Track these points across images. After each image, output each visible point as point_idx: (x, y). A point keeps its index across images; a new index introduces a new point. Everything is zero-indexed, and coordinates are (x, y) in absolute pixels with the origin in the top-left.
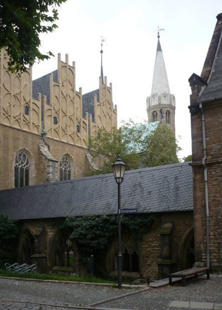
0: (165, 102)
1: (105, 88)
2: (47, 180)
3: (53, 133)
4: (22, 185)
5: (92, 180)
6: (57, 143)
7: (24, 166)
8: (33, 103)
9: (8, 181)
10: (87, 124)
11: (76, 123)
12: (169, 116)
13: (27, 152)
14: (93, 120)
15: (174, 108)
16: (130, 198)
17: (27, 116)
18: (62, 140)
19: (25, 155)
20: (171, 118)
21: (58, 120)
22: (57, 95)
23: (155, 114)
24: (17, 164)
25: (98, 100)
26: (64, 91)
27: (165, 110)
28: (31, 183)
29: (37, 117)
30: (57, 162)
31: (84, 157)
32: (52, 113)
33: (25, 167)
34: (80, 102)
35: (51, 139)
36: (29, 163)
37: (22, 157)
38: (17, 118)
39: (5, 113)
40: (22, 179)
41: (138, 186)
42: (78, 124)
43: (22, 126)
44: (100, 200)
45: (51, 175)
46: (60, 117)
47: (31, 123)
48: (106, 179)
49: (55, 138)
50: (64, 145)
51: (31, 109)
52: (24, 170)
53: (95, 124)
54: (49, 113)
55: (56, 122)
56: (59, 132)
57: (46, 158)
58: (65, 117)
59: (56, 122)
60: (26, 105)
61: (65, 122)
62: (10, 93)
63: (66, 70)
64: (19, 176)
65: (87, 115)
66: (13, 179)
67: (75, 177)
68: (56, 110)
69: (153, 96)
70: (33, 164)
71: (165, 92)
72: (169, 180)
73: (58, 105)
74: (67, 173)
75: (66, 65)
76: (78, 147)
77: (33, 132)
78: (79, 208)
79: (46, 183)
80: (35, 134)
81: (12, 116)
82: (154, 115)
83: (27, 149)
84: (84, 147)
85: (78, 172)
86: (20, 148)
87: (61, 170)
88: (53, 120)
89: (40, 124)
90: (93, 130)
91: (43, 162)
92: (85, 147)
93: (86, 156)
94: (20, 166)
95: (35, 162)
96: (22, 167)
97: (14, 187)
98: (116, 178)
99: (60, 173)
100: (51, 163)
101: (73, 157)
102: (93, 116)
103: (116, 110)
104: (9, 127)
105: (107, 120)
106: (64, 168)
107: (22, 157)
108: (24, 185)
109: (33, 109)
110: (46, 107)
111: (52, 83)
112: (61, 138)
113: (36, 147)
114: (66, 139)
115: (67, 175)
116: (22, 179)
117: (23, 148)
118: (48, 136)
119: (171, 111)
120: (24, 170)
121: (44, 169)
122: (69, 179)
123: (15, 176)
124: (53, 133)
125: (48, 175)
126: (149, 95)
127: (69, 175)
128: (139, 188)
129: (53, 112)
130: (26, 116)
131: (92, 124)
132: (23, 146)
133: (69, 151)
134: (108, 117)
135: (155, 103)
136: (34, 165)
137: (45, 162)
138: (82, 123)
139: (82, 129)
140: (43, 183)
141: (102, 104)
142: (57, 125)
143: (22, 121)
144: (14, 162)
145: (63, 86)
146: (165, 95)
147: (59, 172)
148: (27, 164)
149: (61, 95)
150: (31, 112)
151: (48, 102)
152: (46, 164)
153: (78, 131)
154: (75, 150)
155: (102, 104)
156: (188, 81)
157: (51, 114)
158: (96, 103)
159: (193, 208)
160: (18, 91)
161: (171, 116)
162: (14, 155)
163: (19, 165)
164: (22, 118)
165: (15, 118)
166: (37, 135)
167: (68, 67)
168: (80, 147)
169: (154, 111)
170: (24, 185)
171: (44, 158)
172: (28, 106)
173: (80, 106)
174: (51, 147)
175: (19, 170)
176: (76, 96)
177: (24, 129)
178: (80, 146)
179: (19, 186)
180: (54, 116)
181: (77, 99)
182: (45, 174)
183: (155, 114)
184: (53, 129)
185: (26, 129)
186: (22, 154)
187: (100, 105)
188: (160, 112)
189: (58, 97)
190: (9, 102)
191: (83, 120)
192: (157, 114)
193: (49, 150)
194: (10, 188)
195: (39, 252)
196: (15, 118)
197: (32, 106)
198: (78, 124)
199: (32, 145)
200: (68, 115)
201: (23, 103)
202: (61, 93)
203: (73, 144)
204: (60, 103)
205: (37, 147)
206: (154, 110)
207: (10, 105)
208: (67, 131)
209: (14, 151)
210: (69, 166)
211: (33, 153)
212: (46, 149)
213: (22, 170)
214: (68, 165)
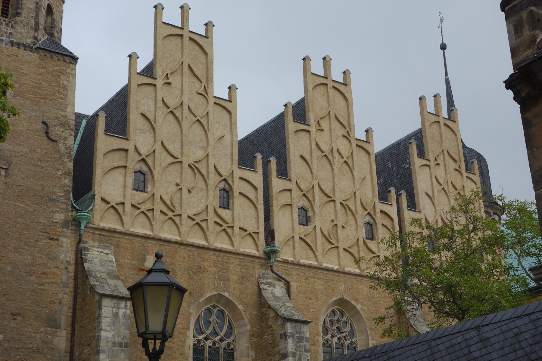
1: (438, 122)
8: (240, 178)
11: (363, 218)
13: (229, 303)
17: (228, 212)
18: (326, 265)
19: (222, 312)
21: (310, 214)
22: (305, 155)
24: (201, 337)
25: (422, 154)
26: (323, 140)
29: (252, 211)
32: (292, 198)
34: (371, 164)
35: (293, 264)
38: (198, 219)
39: (165, 210)
42: (368, 218)
43: (211, 238)
47: (237, 229)
49: (302, 261)
50: (331, 276)
51: (236, 194)
52: (221, 352)
53: (416, 215)
54: (285, 198)
57: (277, 316)
58: (331, 205)
60: (222, 185)
62: (181, 162)
63: (328, 92)
73: (310, 175)
75: (324, 81)
77: (243, 250)
80: (247, 255)
81: (184, 216)
83: (226, 294)
86: (209, 295)
87: (327, 345)
89: (262, 230)
91: (270, 327)
95: (249, 327)
96: (214, 343)
101: (359, 307)
104: (177, 243)
109: (240, 193)
110: (277, 184)
111: (292, 126)
112: (320, 257)
113: (252, 289)
117: (214, 293)
118: (285, 255)
121: (275, 345)
129: (296, 193)
130: (224, 213)
131: (408, 215)
132: (215, 289)
141: (432, 163)
142: (310, 228)
143: (211, 225)
144: (190, 333)
145: (322, 130)
149: (316, 153)
150: (238, 202)
151: (283, 173)
152: (279, 332)
153: (371, 237)
157: (289, 202)
158: (417, 162)
160: (199, 154)
162: (190, 314)
164: (212, 217)
165: (194, 220)
166: (252, 256)
167: (331, 84)
171: (272, 315)
172: (227, 187)
173: (371, 173)
174: (293, 285)
176: (356, 150)
177: (219, 245)
180: (300, 204)
181: (360, 155)
184: (297, 238)
185: (223, 244)
187: (429, 166)
189: (308, 158)
190: (178, 181)
191: (380, 206)
196: (194, 220)
197: (238, 186)
198: (368, 218)
199: (241, 283)
200: (339, 198)
201: (213, 179)
202: (314, 147)
204: (315, 172)
205: (255, 287)
207: (181, 189)
208: (338, 241)
211: (242, 303)
212: (279, 290)
213: (214, 350)
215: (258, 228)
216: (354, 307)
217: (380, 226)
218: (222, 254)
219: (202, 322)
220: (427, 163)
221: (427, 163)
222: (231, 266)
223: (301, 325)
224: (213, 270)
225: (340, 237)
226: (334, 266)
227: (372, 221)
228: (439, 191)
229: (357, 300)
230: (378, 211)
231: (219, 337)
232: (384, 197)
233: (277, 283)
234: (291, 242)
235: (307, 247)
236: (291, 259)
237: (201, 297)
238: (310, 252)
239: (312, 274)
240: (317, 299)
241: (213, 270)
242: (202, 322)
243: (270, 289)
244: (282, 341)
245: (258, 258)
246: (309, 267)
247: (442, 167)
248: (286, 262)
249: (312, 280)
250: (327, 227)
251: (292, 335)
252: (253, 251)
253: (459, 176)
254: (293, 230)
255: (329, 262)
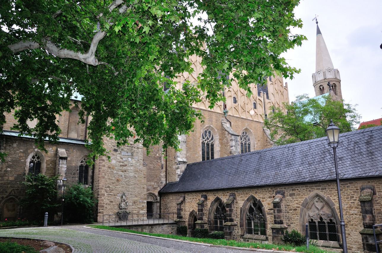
0: (330, 76)
2: (231, 153)
3: (233, 110)
4: (208, 158)
5: (279, 150)
6: (237, 119)
7: (210, 141)
9: (197, 155)
10: (263, 101)
11: (253, 101)
12: (335, 88)
13: (212, 129)
14: (268, 97)
15: (339, 81)
16: (320, 165)
18: (242, 117)
20: (338, 90)
21: (237, 100)
23: (322, 87)
24: (204, 140)
27: (331, 83)
28: (216, 156)
30: (239, 136)
31: (262, 130)
33: (211, 142)
36: (214, 138)
37: (208, 134)
40: (246, 149)
41: (326, 153)
42: (254, 102)
44: (289, 168)
45: (233, 148)
46: (239, 98)
48: (292, 148)
49: (235, 115)
53: (269, 101)
55: (235, 102)
56: (239, 110)
59: (235, 102)
61: (243, 101)
64: (206, 150)
65: (262, 94)
66: (201, 153)
67: (255, 149)
68: (235, 91)
69: (318, 72)
70: (217, 139)
71: (329, 68)
72: (360, 146)
74: (247, 146)
76: (256, 121)
78: (269, 177)
79: (230, 155)
80: (218, 113)
82: (321, 88)
83: (212, 126)
84: (261, 121)
85: (257, 144)
86: (207, 126)
87: (242, 144)
88: (233, 100)
90: (268, 106)
91: (226, 137)
92: (262, 121)
93: (264, 130)
94: (206, 142)
95: (219, 137)
96: (208, 142)
97: (201, 160)
98: (329, 143)
99: (241, 146)
100: (233, 137)
101: (252, 131)
102: (267, 94)
103: (286, 87)
105: (280, 95)
106: (244, 142)
107: (208, 134)
108: (210, 158)
112: (240, 114)
114: (244, 115)
115: (247, 148)
116: (246, 149)
117: (208, 125)
119: (337, 84)
120: (210, 145)
122: (249, 151)
123: (202, 150)
124: (233, 110)
125: (231, 148)
126: (314, 71)
127: (249, 147)
128: (328, 155)
131: (267, 101)
132: (208, 124)
133: (248, 125)
134: (280, 93)
135: (320, 78)
136: (218, 140)
137: (229, 137)
138: (258, 101)
139: (258, 106)
140: (227, 156)
141: (274, 83)
142: (237, 104)
144: (201, 138)
146: (330, 71)
147: (240, 144)
148: (212, 139)
152: (229, 139)
153: (255, 108)
154: (254, 125)
155: (274, 83)
156: (380, 47)
159: (336, 178)
161: (337, 88)
163: (205, 140)
168: (258, 122)
169: (321, 85)
170: (210, 158)
175: (206, 145)
178: (257, 120)
179: (206, 159)
182: (229, 147)
183: (322, 87)
186: (208, 132)
188: (328, 85)
191: (258, 97)
192: (323, 88)
193: (231, 126)
194: (198, 161)
195: (232, 220)
198: (254, 102)
199: (216, 122)
203: (251, 119)
205: (221, 124)
206: (320, 84)
208: (245, 109)
209: (201, 129)
210: (249, 139)
211: (217, 129)
212: (228, 125)
214: (248, 138)
215: (221, 104)
216: (250, 131)
217: (258, 104)
218: (210, 112)
219: (204, 135)
220: (272, 83)
221: (272, 83)
222: (213, 117)
223: (237, 136)
224: (208, 118)
225: (246, 107)
226: (245, 118)
227: (255, 102)
228: (276, 93)
229: (251, 129)
230: (258, 99)
231: (209, 140)
232: (259, 95)
233: (227, 122)
234: (231, 109)
235: (236, 111)
236: (231, 115)
237: (204, 127)
238: (237, 112)
239: (237, 120)
240: (239, 128)
241: (208, 118)
242: (204, 135)
243: (225, 124)
244: (231, 142)
245: (221, 114)
246: (237, 117)
247: (277, 85)
248: (230, 115)
249: (237, 122)
250: (242, 104)
251: (234, 140)
252: (220, 112)
253: (282, 88)
254: (232, 105)
255: (244, 116)
